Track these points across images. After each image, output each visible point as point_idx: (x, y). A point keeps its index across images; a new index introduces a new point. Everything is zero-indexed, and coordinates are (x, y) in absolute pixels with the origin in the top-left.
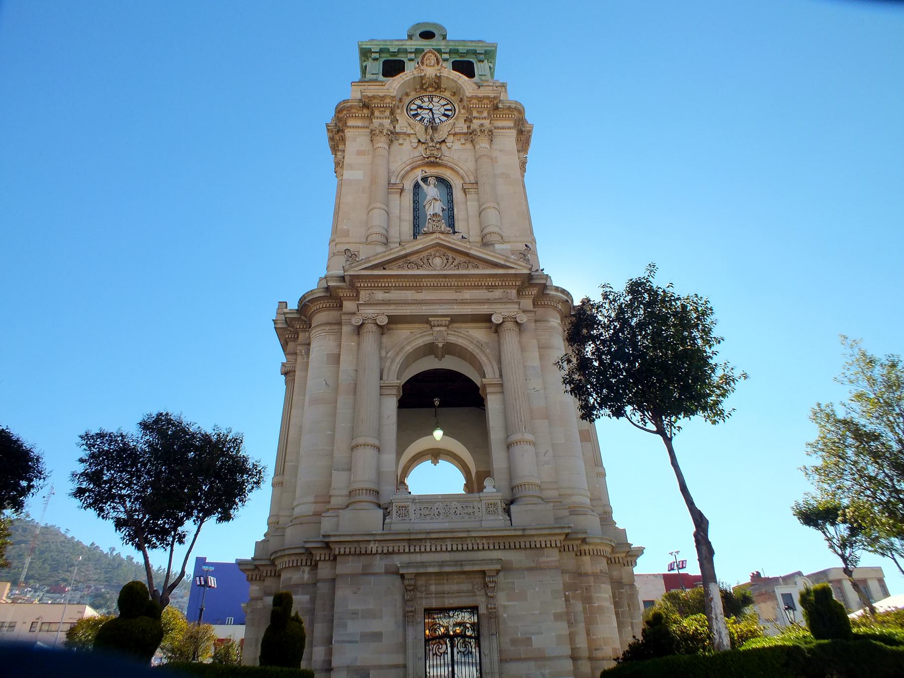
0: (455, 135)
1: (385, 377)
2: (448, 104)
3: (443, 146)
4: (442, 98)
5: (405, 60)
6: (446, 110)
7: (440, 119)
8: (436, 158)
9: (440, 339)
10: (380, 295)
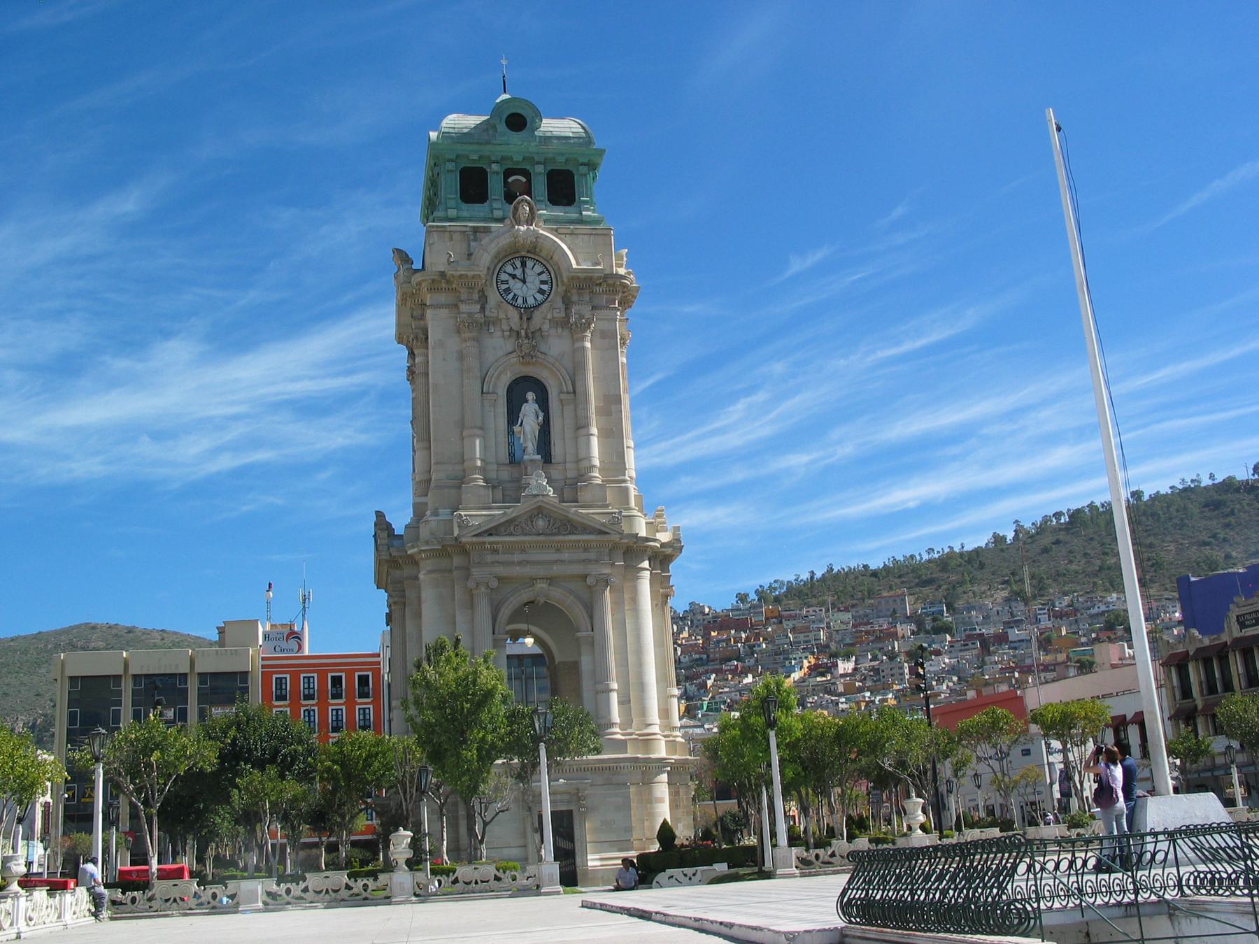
1: (496, 631)
2: (543, 272)
5: (488, 170)
6: (543, 282)
10: (489, 558)
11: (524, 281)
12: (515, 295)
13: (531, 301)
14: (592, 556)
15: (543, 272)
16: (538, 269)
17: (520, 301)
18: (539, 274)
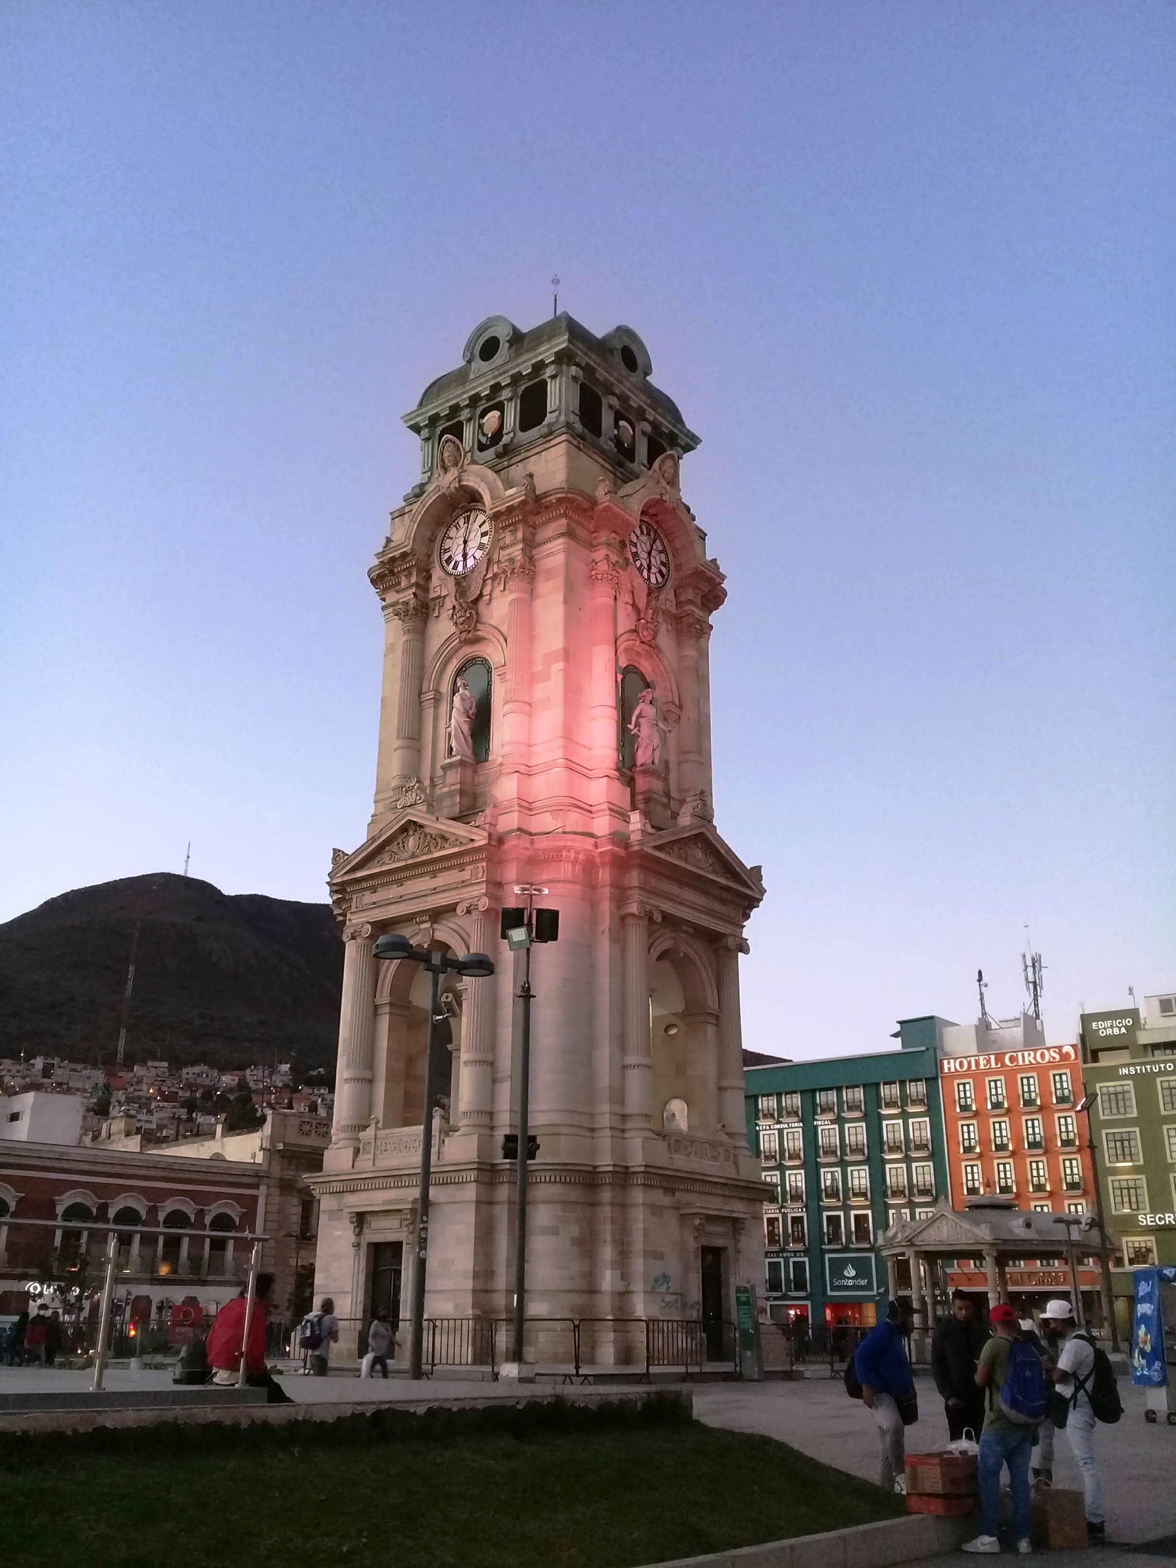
2: (484, 522)
3: (482, 605)
7: (474, 557)
8: (470, 631)
9: (425, 939)
10: (368, 898)
12: (456, 562)
14: (466, 875)
15: (484, 522)
17: (460, 568)
18: (480, 526)
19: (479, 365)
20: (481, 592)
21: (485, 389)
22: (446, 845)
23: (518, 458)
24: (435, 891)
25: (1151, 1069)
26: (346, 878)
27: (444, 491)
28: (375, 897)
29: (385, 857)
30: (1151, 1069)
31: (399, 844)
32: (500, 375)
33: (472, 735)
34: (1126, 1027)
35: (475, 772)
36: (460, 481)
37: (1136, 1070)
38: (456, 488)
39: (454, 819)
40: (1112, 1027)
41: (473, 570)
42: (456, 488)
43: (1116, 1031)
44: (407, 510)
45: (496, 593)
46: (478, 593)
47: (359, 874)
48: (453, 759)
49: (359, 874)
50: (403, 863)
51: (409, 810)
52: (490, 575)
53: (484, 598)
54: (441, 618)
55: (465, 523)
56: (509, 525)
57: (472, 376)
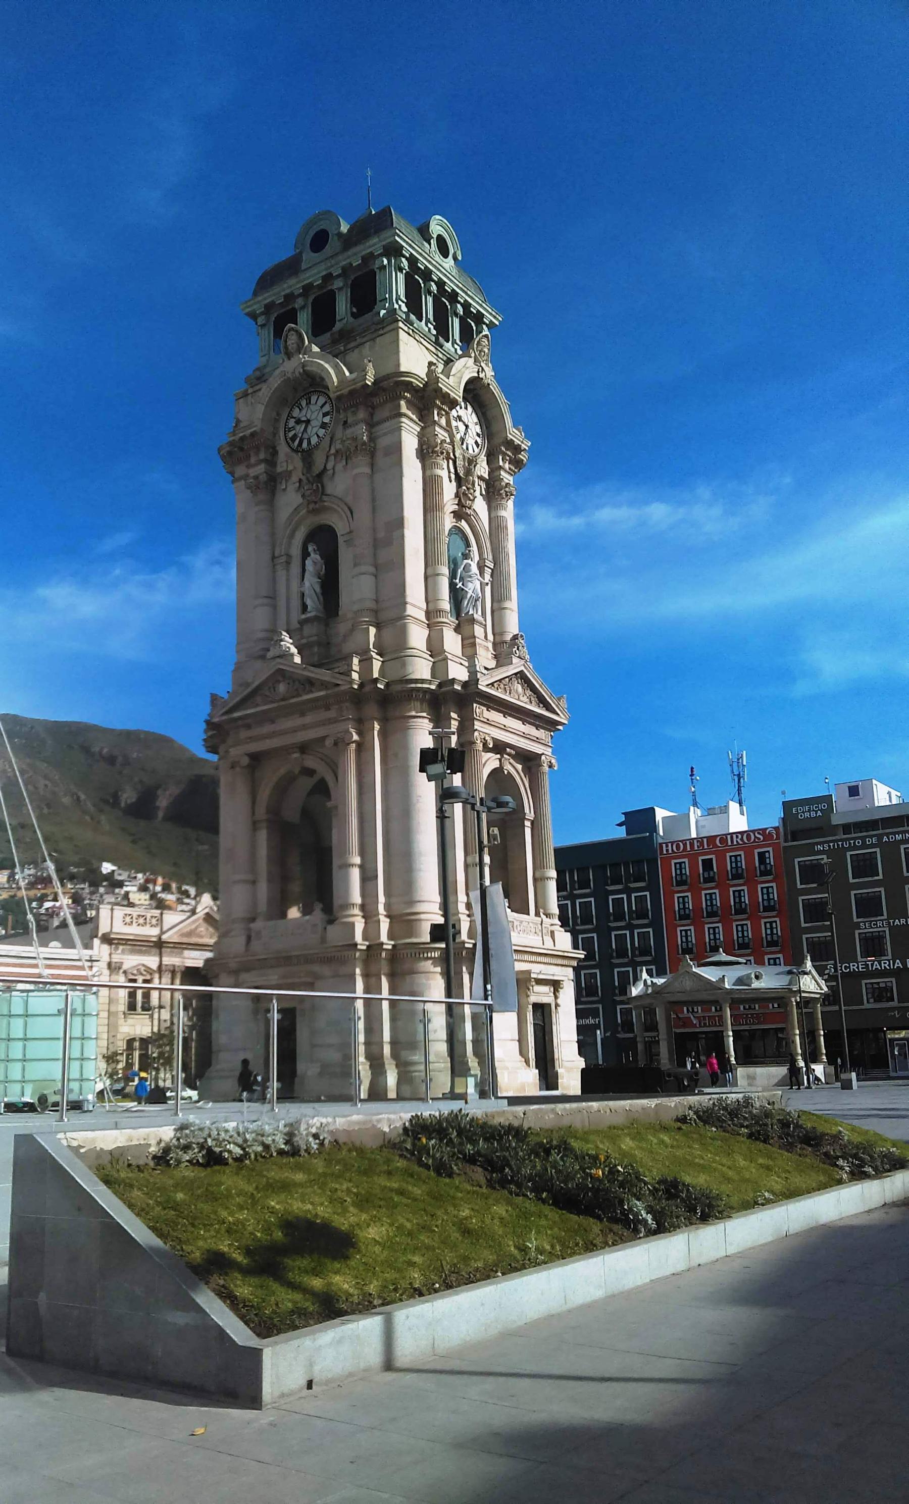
0: (335, 455)
2: (326, 403)
3: (325, 480)
4: (320, 392)
7: (318, 436)
10: (244, 734)
11: (308, 422)
13: (314, 440)
15: (326, 403)
16: (322, 400)
17: (305, 445)
18: (322, 407)
19: (308, 257)
20: (325, 467)
21: (315, 281)
22: (313, 689)
23: (352, 345)
24: (304, 727)
25: (842, 844)
26: (224, 718)
27: (289, 375)
28: (250, 733)
29: (258, 699)
30: (842, 844)
31: (270, 688)
32: (332, 266)
33: (322, 594)
34: (821, 810)
35: (327, 625)
36: (303, 367)
37: (829, 846)
38: (300, 373)
39: (314, 666)
40: (809, 811)
41: (317, 446)
42: (300, 373)
43: (813, 814)
44: (250, 391)
45: (340, 466)
46: (322, 467)
47: (236, 715)
48: (309, 615)
49: (236, 715)
50: (275, 705)
51: (279, 660)
52: (333, 451)
53: (329, 472)
54: (288, 489)
55: (307, 404)
56: (352, 407)
57: (304, 266)
